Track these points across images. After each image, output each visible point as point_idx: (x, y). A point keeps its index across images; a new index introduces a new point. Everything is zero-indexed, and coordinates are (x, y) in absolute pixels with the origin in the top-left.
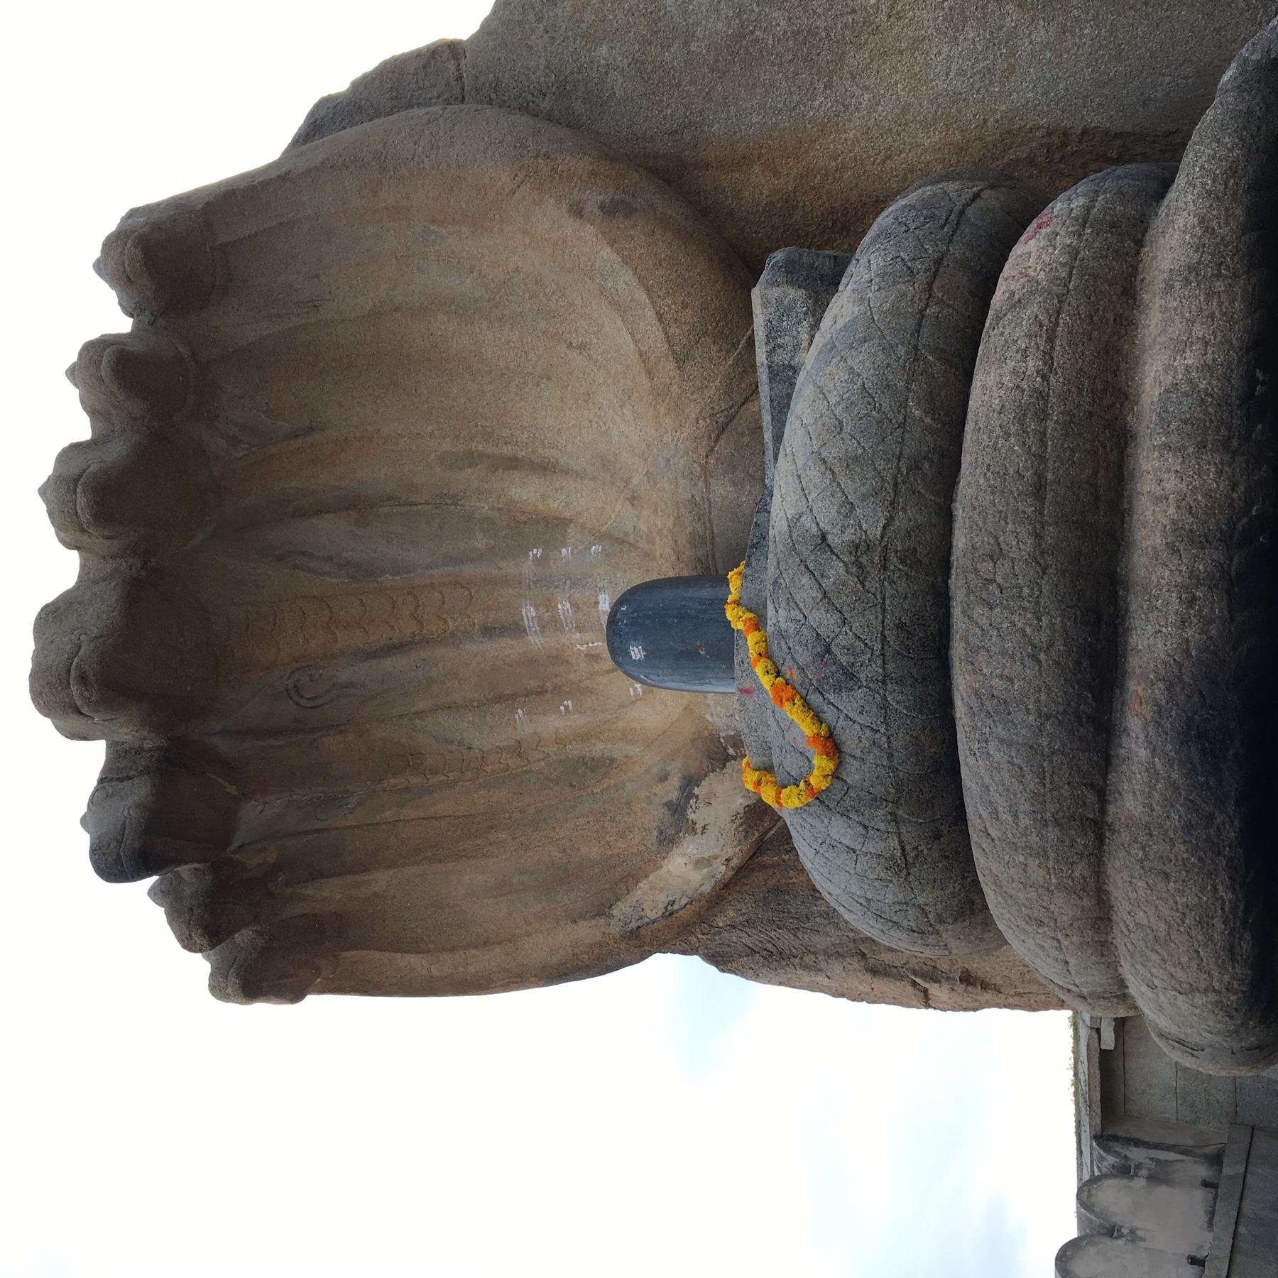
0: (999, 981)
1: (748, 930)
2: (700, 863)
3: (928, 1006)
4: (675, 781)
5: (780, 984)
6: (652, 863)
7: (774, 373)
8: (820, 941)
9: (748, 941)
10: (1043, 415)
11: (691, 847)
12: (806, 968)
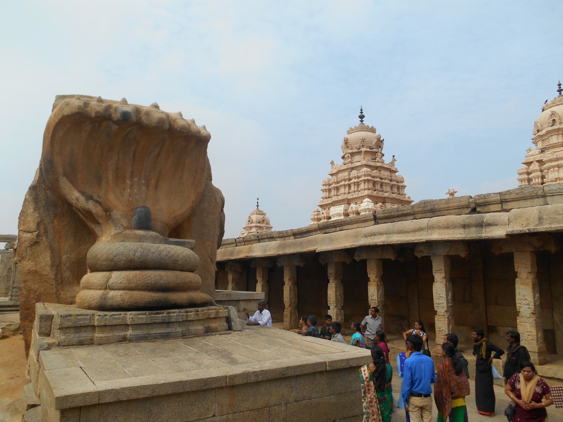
0: (34, 247)
1: (45, 197)
2: (77, 199)
3: (19, 231)
4: (98, 199)
5: (26, 200)
6: (77, 188)
7: (184, 242)
8: (42, 211)
9: (41, 196)
10: (191, 283)
11: (82, 199)
12: (35, 207)
